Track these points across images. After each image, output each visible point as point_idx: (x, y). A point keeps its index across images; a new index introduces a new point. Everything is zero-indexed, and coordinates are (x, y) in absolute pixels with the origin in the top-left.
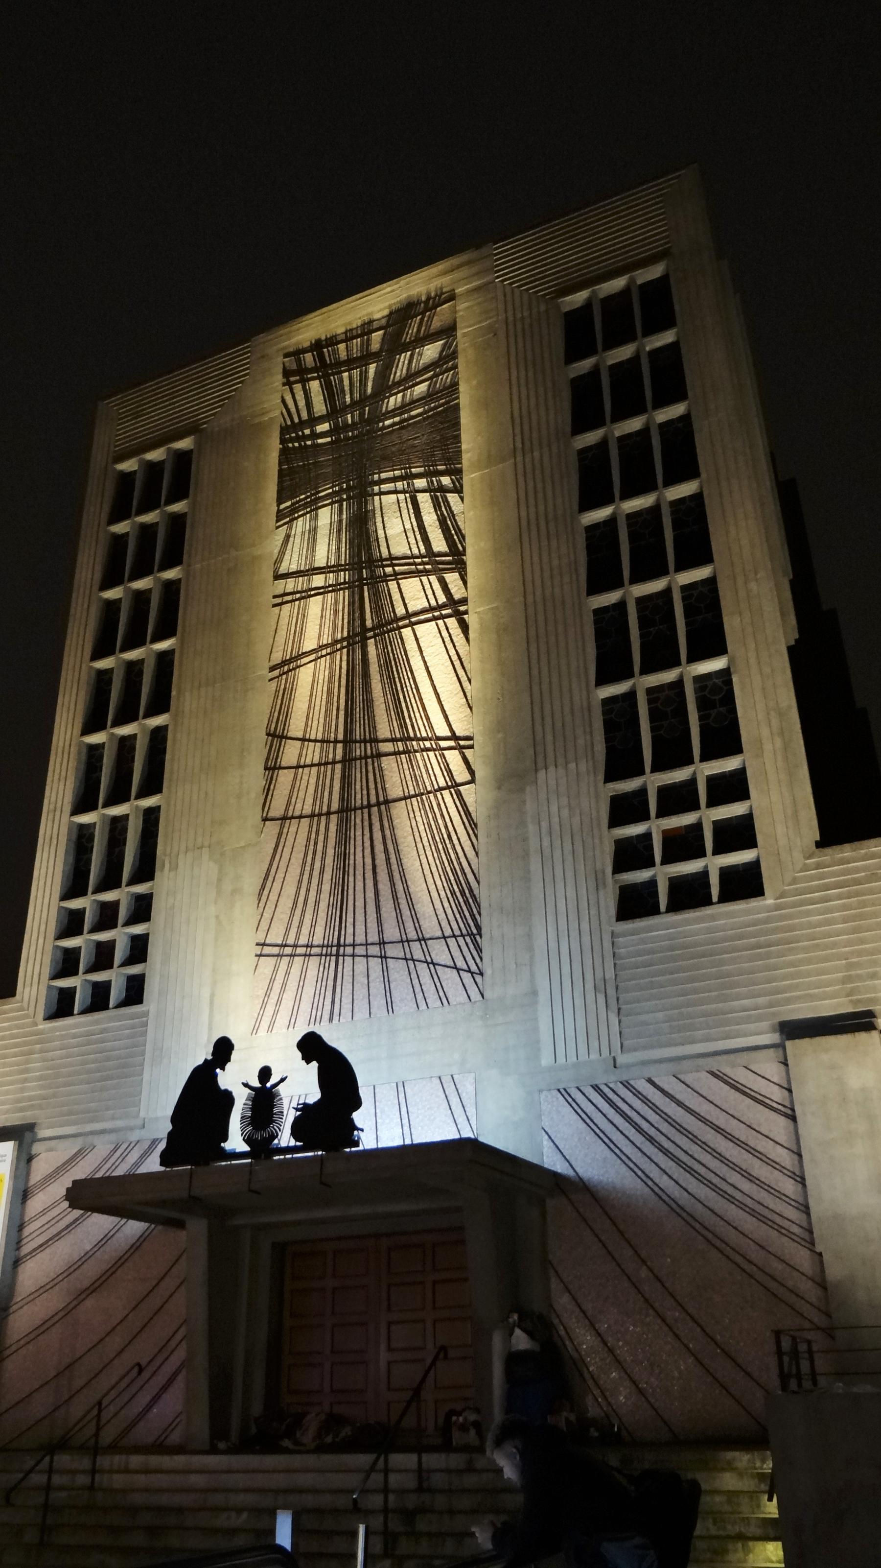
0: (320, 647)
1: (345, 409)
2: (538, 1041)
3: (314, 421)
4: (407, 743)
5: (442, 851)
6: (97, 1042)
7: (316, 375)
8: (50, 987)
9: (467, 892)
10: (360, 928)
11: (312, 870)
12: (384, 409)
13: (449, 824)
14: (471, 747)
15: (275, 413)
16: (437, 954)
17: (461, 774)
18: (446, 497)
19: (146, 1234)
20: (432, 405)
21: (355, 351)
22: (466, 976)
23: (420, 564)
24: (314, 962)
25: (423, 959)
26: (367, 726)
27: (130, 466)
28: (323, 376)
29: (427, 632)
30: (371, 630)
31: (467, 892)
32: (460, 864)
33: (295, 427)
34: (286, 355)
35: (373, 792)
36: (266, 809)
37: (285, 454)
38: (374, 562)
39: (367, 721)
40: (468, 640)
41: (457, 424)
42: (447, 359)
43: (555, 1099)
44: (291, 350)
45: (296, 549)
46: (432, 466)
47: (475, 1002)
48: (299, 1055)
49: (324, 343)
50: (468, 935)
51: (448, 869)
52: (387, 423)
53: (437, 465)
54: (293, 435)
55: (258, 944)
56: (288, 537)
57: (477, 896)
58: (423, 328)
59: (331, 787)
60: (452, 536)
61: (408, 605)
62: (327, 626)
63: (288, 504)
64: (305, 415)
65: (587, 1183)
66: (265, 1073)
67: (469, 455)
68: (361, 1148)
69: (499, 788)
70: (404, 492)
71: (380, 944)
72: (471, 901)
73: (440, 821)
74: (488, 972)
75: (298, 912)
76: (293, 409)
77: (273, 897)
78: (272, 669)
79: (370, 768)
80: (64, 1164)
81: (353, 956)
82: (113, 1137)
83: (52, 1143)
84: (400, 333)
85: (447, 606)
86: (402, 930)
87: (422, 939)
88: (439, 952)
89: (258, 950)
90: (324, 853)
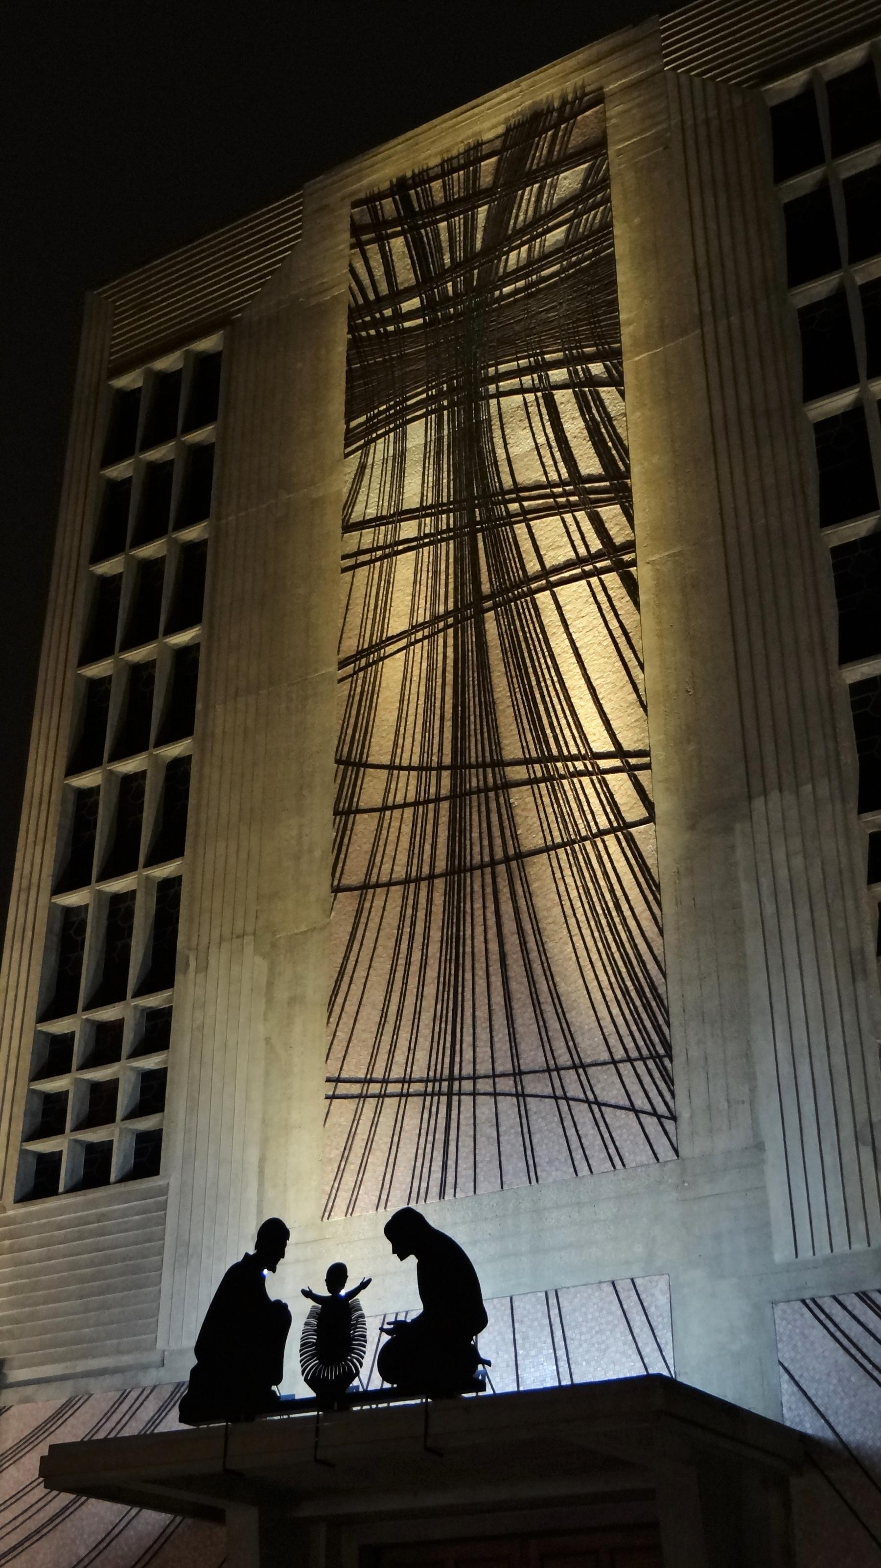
0: (413, 627)
1: (444, 274)
2: (767, 1224)
3: (397, 295)
4: (550, 765)
5: (606, 929)
6: (92, 1234)
7: (400, 228)
8: (23, 1153)
9: (647, 990)
10: (482, 1052)
11: (408, 964)
12: (501, 270)
13: (617, 887)
14: (647, 767)
15: (341, 289)
16: (603, 1089)
17: (631, 808)
18: (598, 393)
19: (168, 1531)
20: (574, 259)
21: (456, 189)
22: (650, 1122)
23: (561, 495)
24: (414, 1105)
25: (582, 1096)
26: (486, 742)
27: (134, 381)
28: (411, 229)
29: (575, 596)
30: (490, 599)
31: (647, 990)
32: (635, 947)
33: (369, 307)
34: (355, 205)
36: (337, 875)
37: (355, 345)
38: (493, 496)
39: (486, 735)
40: (637, 604)
41: (611, 284)
42: (595, 190)
43: (797, 1316)
44: (362, 195)
45: (375, 485)
46: (576, 348)
47: (666, 1162)
48: (389, 1246)
49: (410, 182)
50: (652, 1057)
51: (617, 955)
52: (506, 290)
53: (582, 347)
54: (368, 319)
55: (328, 1080)
56: (362, 468)
57: (664, 997)
58: (557, 148)
59: (435, 835)
60: (609, 449)
61: (545, 558)
62: (423, 595)
63: (363, 419)
64: (384, 289)
65: (855, 1452)
66: (337, 1274)
67: (631, 328)
68: (489, 1391)
69: (692, 828)
70: (533, 390)
71: (514, 1074)
72: (654, 1004)
73: (602, 883)
74: (684, 1114)
75: (389, 1028)
76: (366, 282)
77: (351, 1008)
78: (342, 664)
79: (493, 805)
80: (46, 1422)
81: (474, 1094)
82: (117, 1380)
83: (29, 1390)
84: (522, 158)
85: (604, 555)
86: (549, 1054)
87: (580, 1066)
88: (607, 1086)
89: (329, 1089)
90: (426, 937)
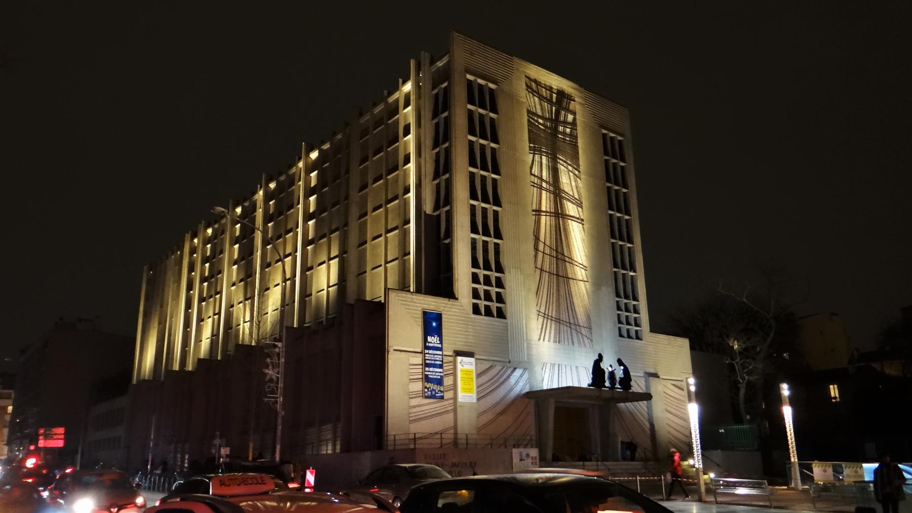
4: (572, 261)
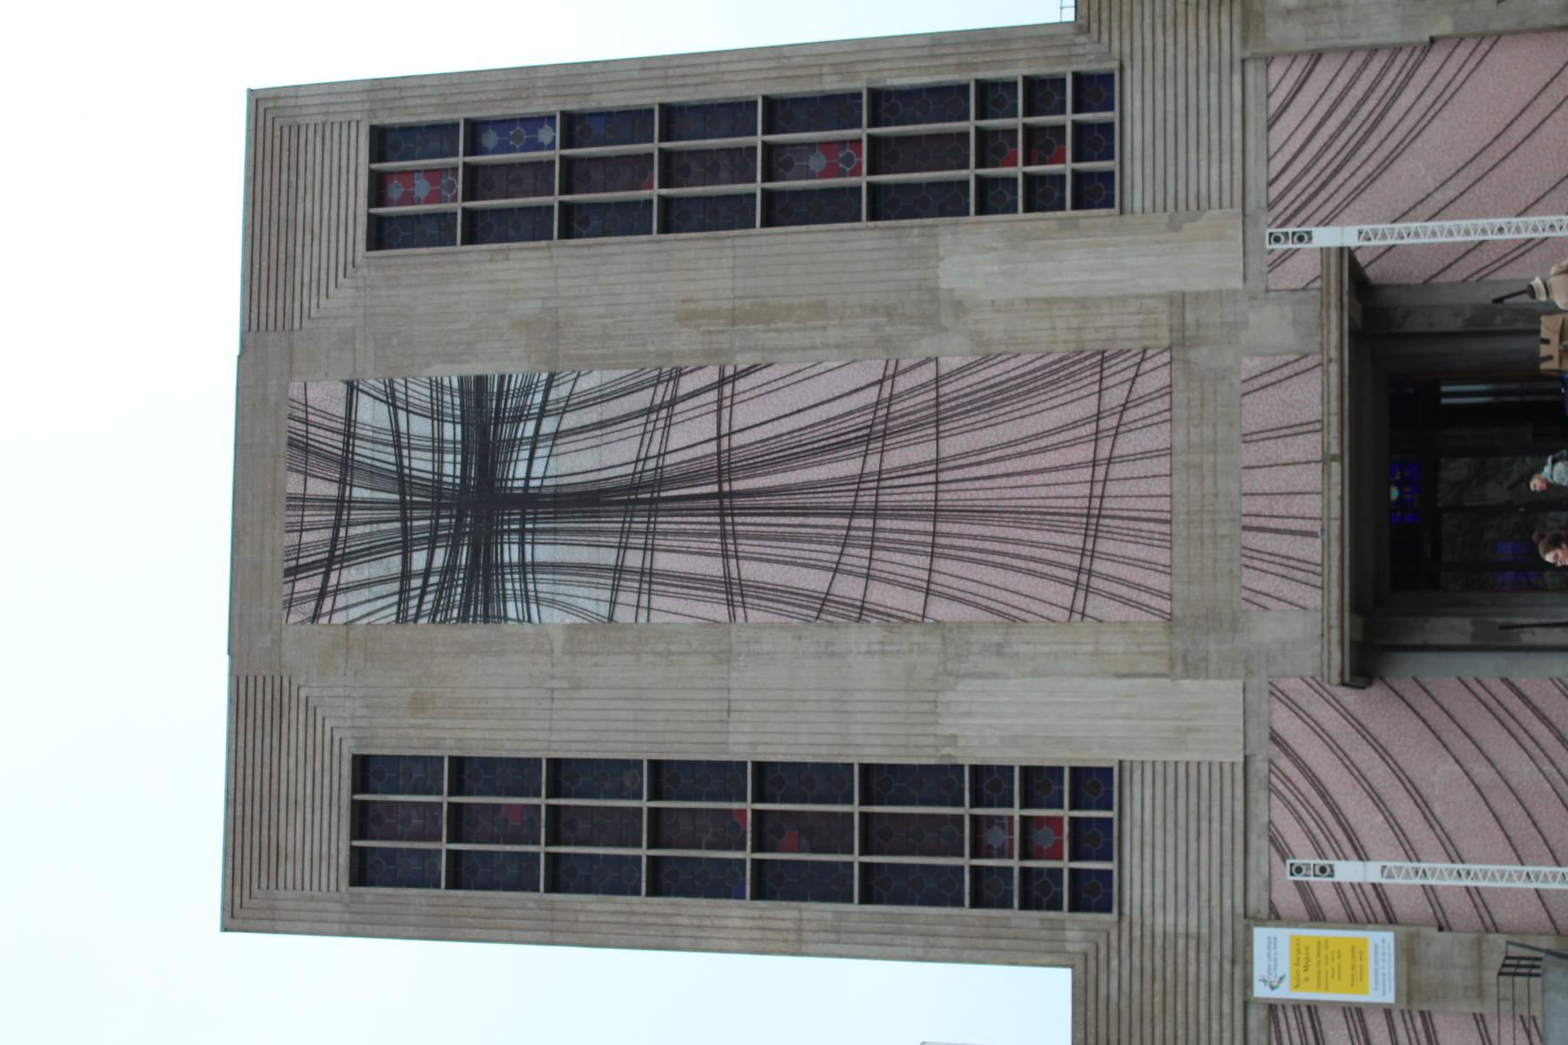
2: (1220, 292)
22: (1146, 366)
35: (924, 479)
81: (1102, 497)
87: (1098, 417)
88: (1115, 397)
89: (1077, 617)
